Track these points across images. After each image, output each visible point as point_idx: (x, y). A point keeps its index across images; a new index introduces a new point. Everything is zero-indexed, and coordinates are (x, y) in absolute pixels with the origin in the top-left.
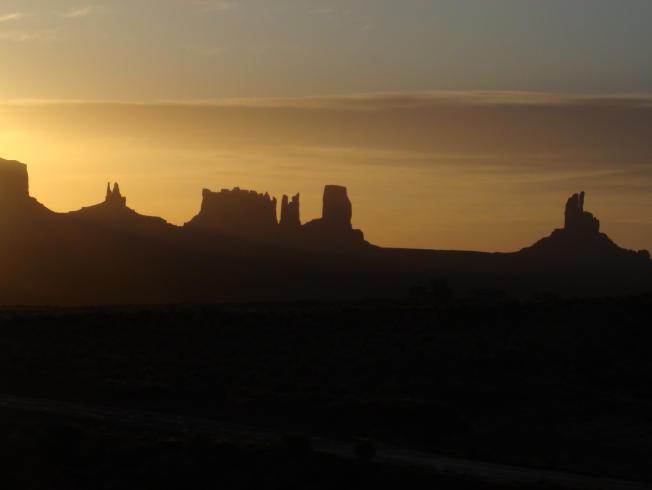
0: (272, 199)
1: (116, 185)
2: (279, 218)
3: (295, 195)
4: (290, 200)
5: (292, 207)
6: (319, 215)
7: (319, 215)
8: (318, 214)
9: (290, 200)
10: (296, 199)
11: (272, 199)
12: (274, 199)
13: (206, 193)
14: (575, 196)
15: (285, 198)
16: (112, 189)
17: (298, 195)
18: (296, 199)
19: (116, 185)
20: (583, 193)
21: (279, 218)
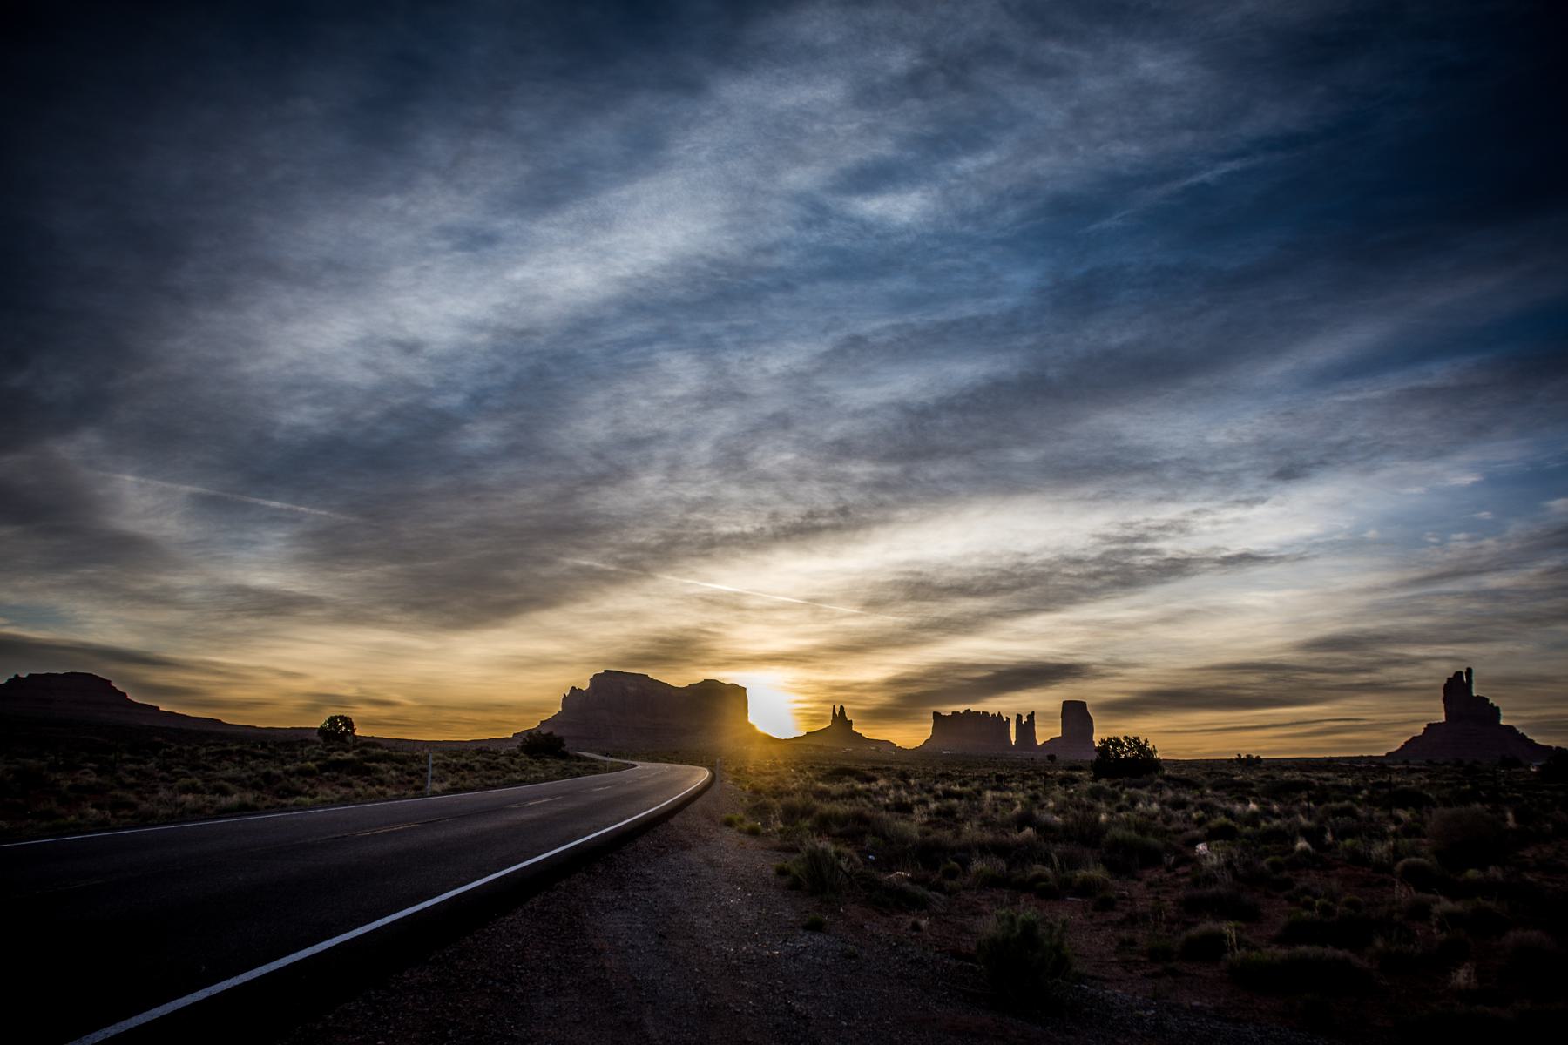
0: (1005, 720)
1: (842, 708)
2: (1013, 739)
3: (1030, 713)
4: (1025, 719)
5: (1027, 726)
6: (1060, 735)
7: (1060, 735)
8: (1057, 732)
9: (1025, 719)
10: (1031, 717)
11: (1005, 720)
12: (1007, 718)
13: (936, 715)
14: (1458, 674)
15: (1019, 717)
16: (837, 713)
17: (1033, 713)
18: (1031, 717)
19: (842, 708)
20: (1469, 671)
21: (1013, 739)
